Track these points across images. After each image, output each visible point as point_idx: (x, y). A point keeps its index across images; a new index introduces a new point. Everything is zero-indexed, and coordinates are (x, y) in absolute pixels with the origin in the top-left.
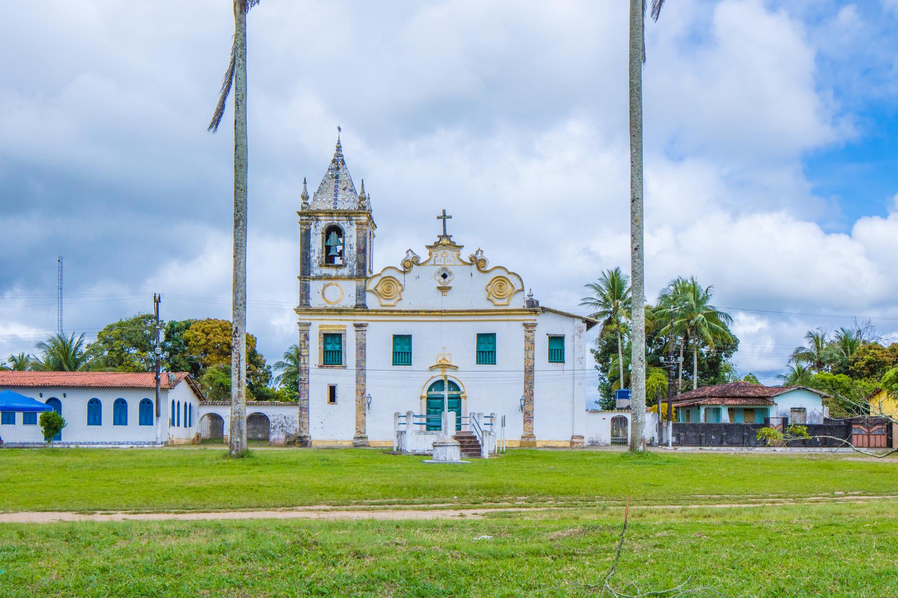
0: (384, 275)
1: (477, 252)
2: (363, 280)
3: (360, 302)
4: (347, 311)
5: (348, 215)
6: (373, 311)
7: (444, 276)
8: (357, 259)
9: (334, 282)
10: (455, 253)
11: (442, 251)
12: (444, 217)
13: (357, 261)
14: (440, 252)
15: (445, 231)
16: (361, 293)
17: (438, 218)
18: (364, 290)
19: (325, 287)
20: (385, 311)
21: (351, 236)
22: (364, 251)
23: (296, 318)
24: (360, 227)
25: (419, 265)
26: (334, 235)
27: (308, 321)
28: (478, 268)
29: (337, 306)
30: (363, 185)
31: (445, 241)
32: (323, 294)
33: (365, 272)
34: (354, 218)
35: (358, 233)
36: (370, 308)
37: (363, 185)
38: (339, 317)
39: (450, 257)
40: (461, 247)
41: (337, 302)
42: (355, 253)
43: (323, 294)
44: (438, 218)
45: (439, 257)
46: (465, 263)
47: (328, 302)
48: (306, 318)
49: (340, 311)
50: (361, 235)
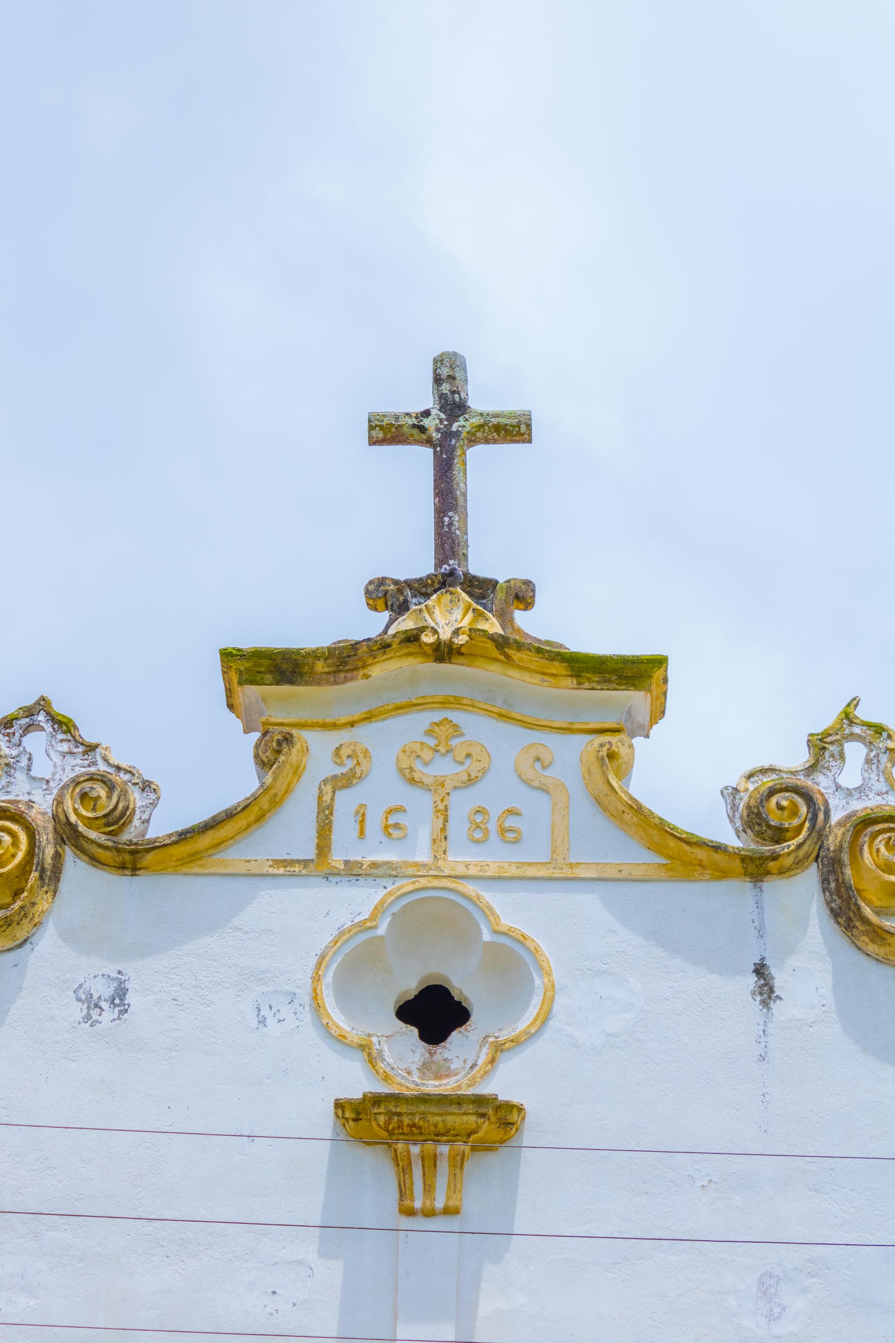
1: (823, 748)
7: (434, 1013)
10: (571, 754)
11: (410, 728)
12: (447, 428)
14: (388, 742)
15: (448, 543)
17: (387, 432)
25: (131, 860)
28: (845, 910)
31: (448, 617)
39: (497, 792)
40: (636, 673)
44: (387, 432)
45: (380, 788)
46: (683, 855)
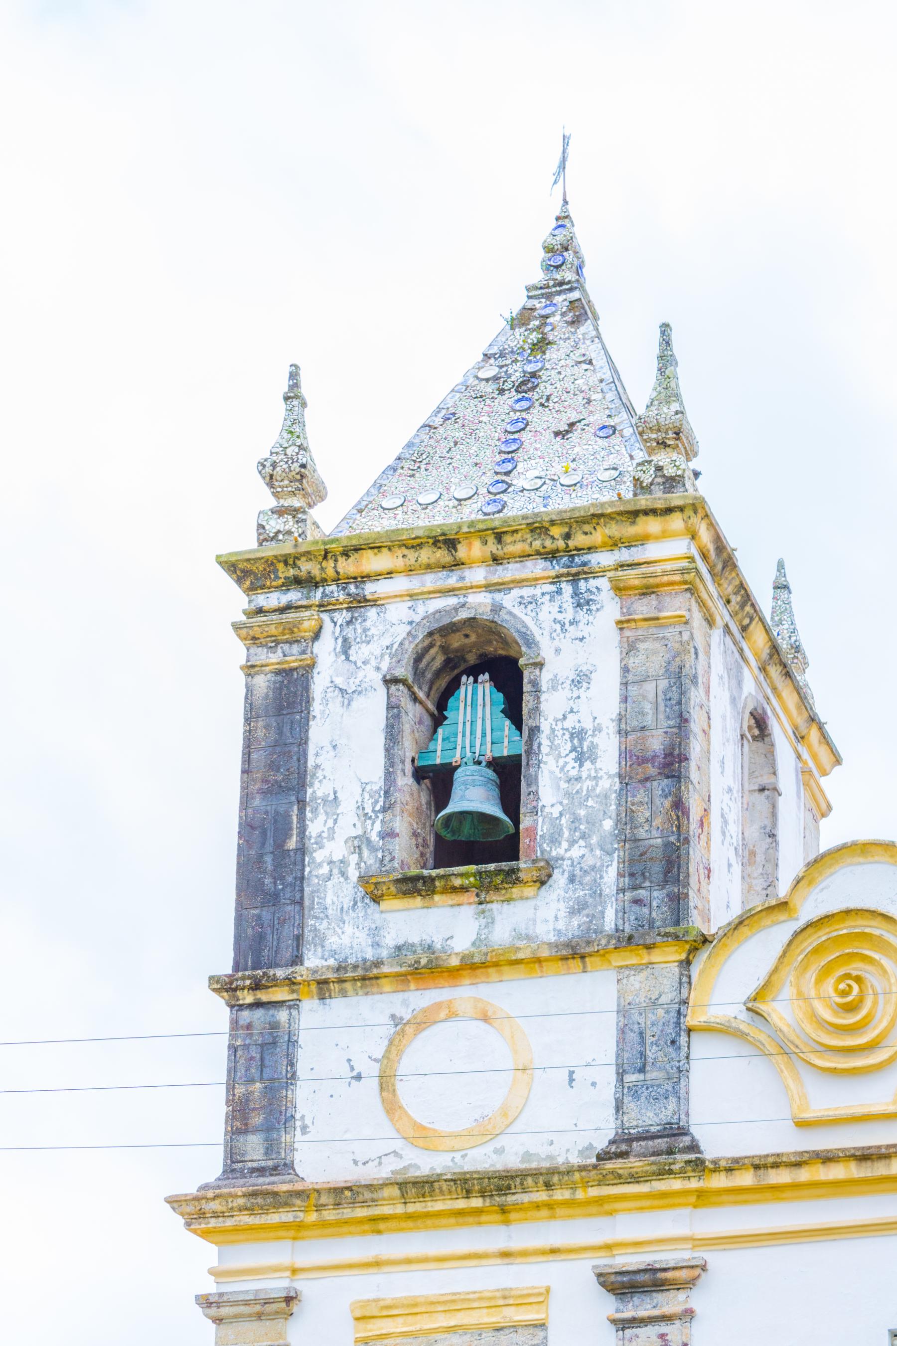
0: (810, 908)
2: (668, 957)
3: (646, 1116)
4: (548, 1177)
5: (563, 545)
6: (733, 1166)
8: (627, 818)
9: (464, 993)
13: (627, 832)
16: (654, 1053)
18: (680, 1031)
19: (404, 1030)
20: (827, 1158)
21: (581, 679)
22: (673, 764)
23: (197, 1262)
24: (643, 608)
26: (478, 700)
27: (276, 1285)
29: (482, 1159)
30: (666, 360)
32: (386, 1083)
33: (678, 903)
34: (604, 559)
35: (630, 648)
36: (715, 1143)
37: (666, 360)
38: (493, 1237)
41: (485, 1132)
42: (609, 784)
43: (386, 1083)
47: (422, 1136)
48: (266, 1263)
49: (497, 1191)
50: (652, 658)
